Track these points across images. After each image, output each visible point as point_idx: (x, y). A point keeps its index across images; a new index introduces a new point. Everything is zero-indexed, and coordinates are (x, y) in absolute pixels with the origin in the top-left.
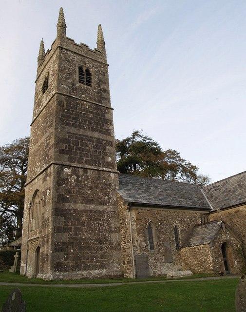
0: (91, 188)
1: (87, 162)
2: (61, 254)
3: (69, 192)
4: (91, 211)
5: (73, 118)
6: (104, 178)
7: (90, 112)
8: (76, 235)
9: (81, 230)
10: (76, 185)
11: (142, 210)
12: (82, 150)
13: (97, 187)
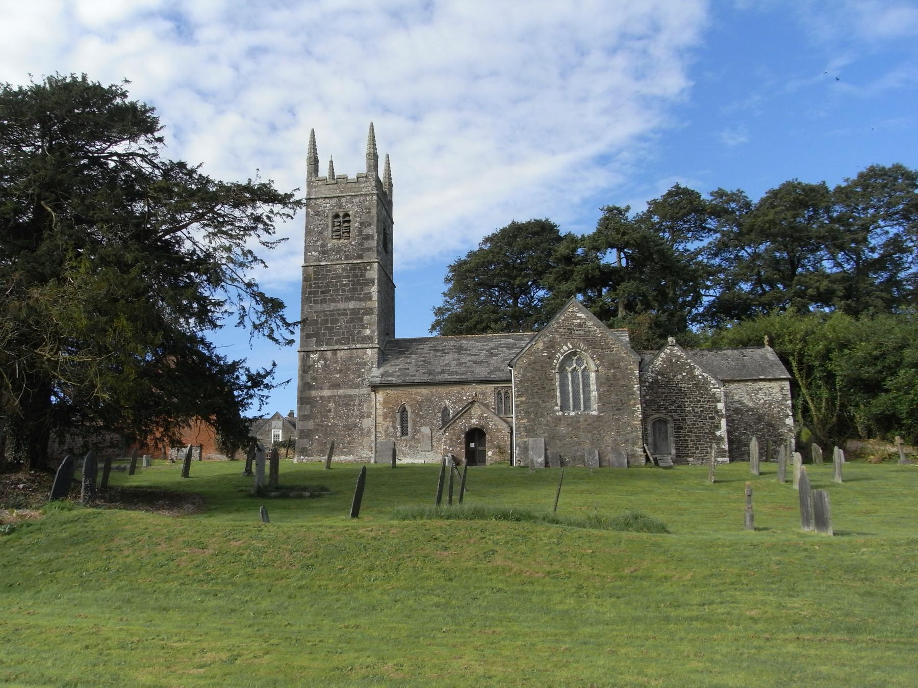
0: (340, 371)
1: (339, 342)
2: (306, 440)
3: (315, 379)
4: (339, 397)
5: (323, 292)
6: (358, 357)
7: (345, 277)
8: (322, 421)
9: (327, 417)
10: (324, 370)
11: (392, 392)
12: (332, 328)
13: (348, 369)
